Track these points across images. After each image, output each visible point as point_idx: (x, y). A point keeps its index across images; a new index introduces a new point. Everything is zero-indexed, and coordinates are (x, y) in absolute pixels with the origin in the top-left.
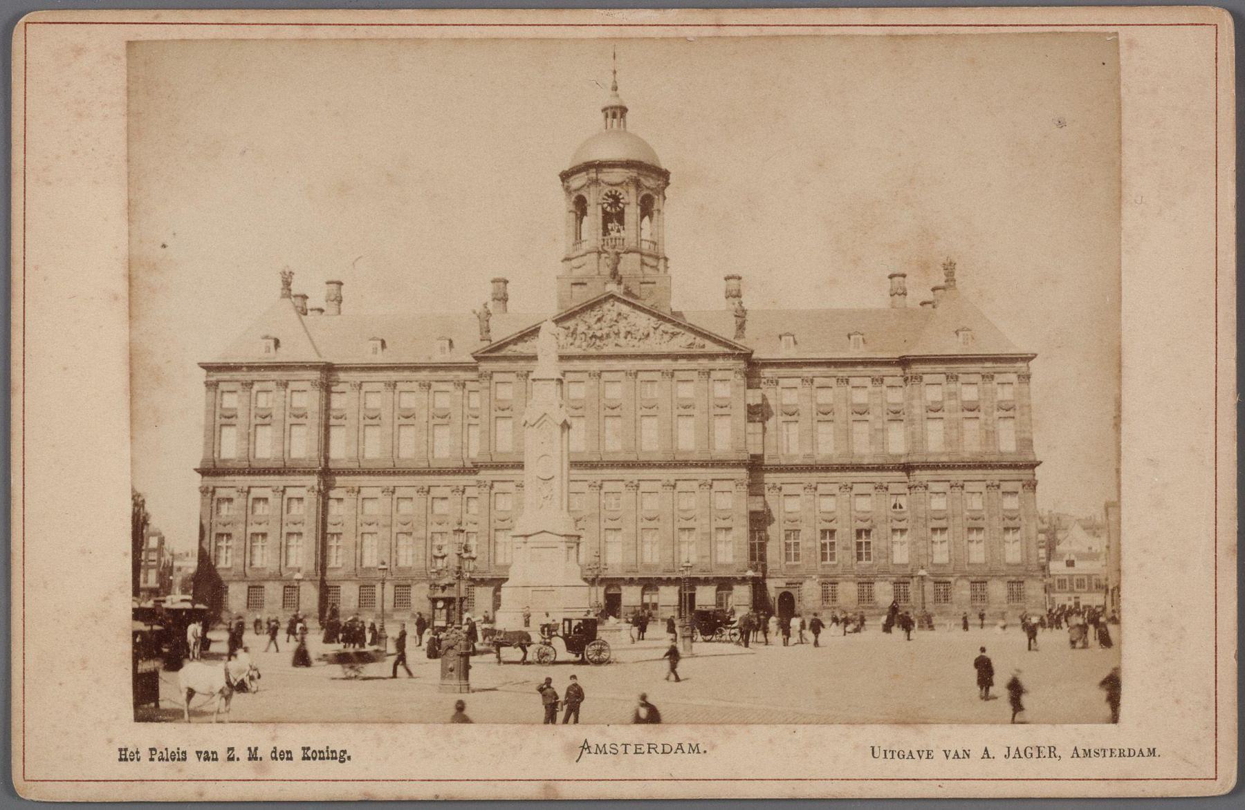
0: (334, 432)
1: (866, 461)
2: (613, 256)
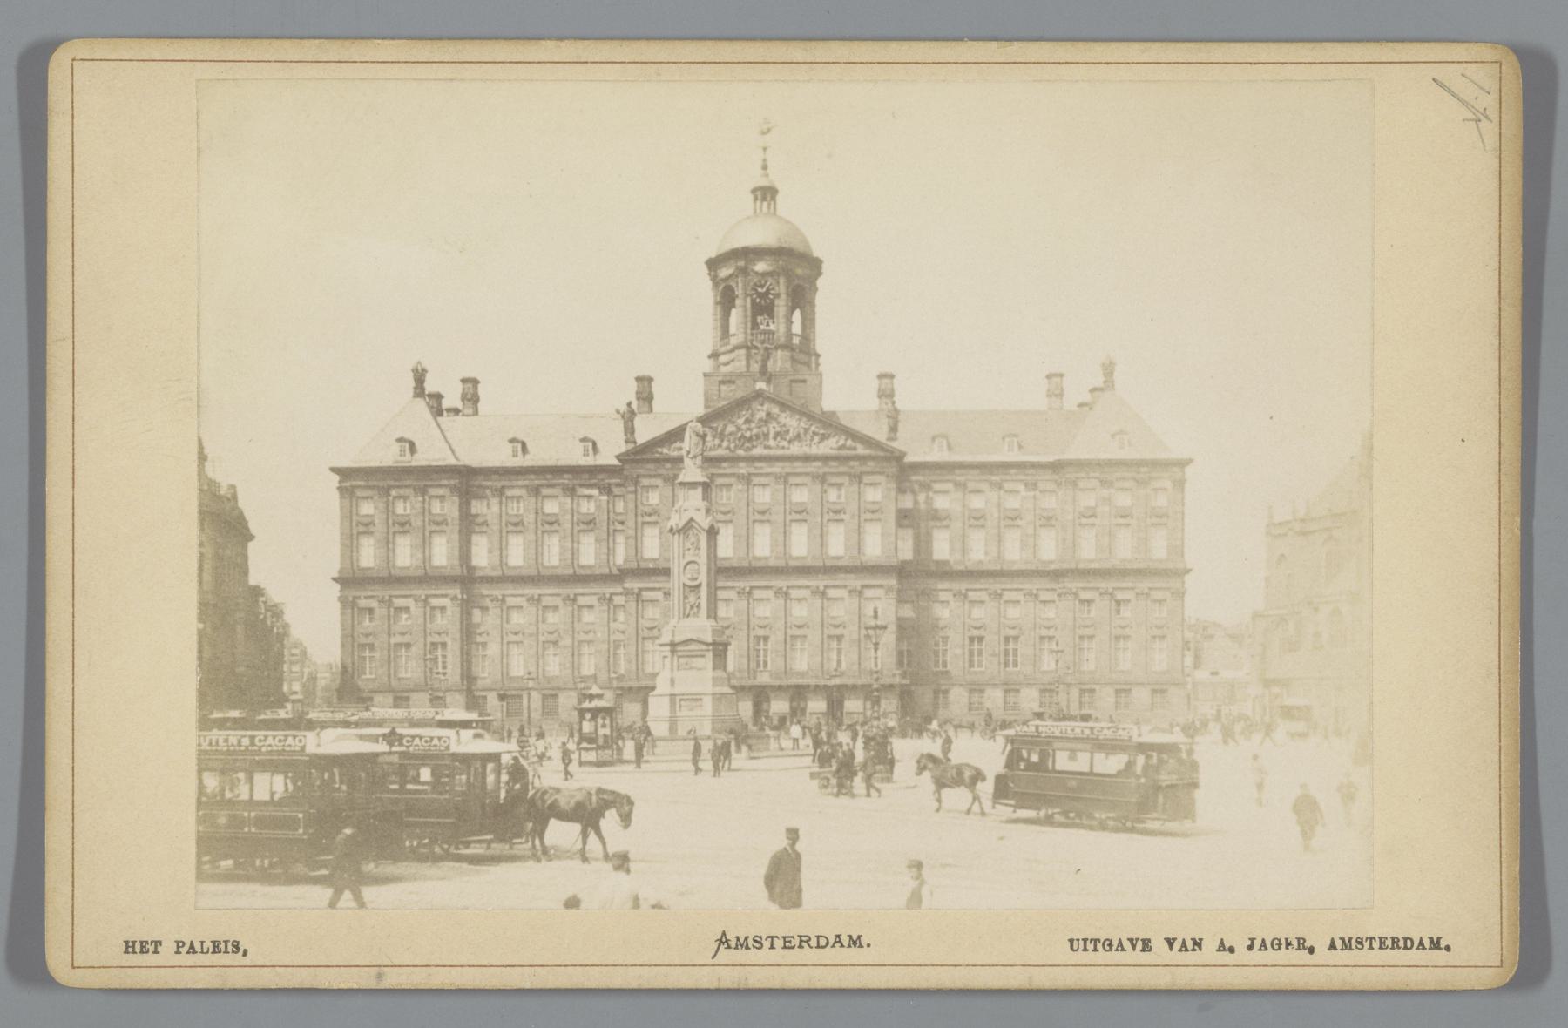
0: (475, 538)
1: (1016, 567)
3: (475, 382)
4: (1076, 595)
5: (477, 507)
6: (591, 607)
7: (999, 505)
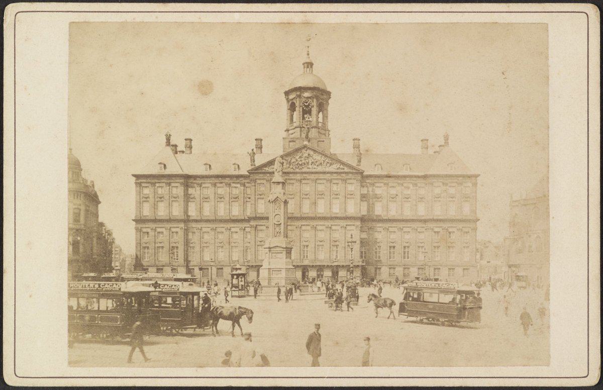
0: (190, 203)
1: (408, 218)
2: (306, 129)
3: (191, 140)
4: (432, 229)
5: (191, 191)
6: (237, 232)
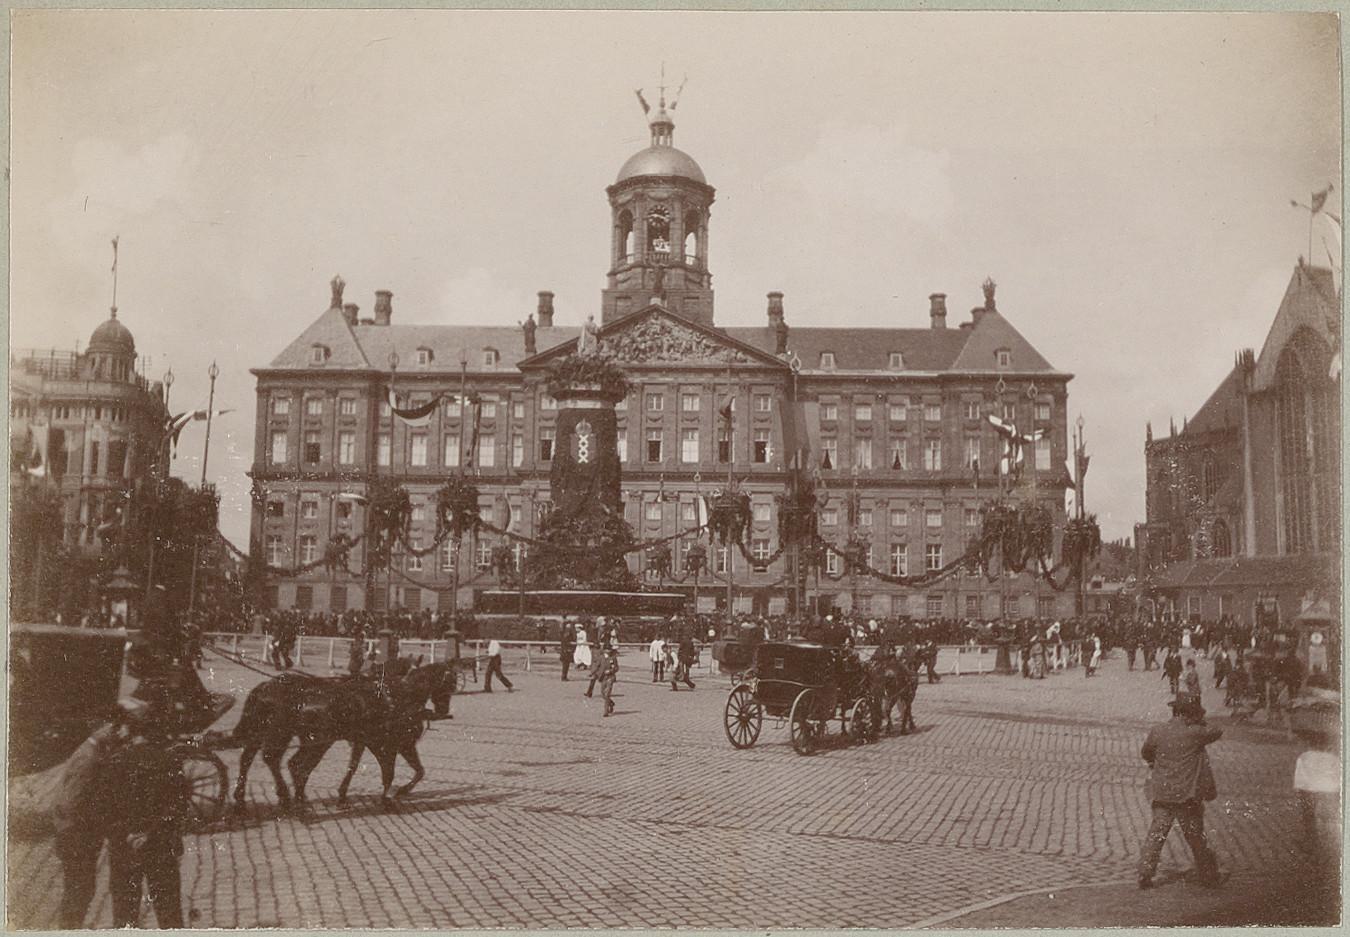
2: (657, 270)
3: (388, 295)
6: (490, 506)
7: (884, 418)
